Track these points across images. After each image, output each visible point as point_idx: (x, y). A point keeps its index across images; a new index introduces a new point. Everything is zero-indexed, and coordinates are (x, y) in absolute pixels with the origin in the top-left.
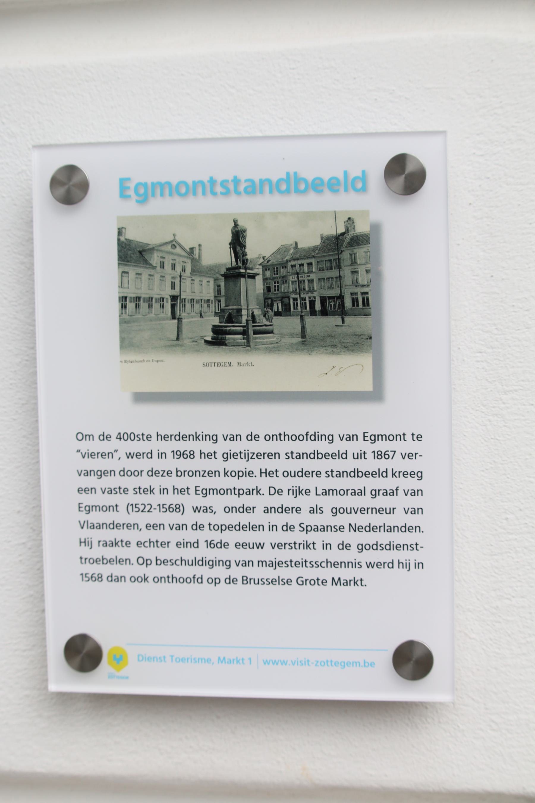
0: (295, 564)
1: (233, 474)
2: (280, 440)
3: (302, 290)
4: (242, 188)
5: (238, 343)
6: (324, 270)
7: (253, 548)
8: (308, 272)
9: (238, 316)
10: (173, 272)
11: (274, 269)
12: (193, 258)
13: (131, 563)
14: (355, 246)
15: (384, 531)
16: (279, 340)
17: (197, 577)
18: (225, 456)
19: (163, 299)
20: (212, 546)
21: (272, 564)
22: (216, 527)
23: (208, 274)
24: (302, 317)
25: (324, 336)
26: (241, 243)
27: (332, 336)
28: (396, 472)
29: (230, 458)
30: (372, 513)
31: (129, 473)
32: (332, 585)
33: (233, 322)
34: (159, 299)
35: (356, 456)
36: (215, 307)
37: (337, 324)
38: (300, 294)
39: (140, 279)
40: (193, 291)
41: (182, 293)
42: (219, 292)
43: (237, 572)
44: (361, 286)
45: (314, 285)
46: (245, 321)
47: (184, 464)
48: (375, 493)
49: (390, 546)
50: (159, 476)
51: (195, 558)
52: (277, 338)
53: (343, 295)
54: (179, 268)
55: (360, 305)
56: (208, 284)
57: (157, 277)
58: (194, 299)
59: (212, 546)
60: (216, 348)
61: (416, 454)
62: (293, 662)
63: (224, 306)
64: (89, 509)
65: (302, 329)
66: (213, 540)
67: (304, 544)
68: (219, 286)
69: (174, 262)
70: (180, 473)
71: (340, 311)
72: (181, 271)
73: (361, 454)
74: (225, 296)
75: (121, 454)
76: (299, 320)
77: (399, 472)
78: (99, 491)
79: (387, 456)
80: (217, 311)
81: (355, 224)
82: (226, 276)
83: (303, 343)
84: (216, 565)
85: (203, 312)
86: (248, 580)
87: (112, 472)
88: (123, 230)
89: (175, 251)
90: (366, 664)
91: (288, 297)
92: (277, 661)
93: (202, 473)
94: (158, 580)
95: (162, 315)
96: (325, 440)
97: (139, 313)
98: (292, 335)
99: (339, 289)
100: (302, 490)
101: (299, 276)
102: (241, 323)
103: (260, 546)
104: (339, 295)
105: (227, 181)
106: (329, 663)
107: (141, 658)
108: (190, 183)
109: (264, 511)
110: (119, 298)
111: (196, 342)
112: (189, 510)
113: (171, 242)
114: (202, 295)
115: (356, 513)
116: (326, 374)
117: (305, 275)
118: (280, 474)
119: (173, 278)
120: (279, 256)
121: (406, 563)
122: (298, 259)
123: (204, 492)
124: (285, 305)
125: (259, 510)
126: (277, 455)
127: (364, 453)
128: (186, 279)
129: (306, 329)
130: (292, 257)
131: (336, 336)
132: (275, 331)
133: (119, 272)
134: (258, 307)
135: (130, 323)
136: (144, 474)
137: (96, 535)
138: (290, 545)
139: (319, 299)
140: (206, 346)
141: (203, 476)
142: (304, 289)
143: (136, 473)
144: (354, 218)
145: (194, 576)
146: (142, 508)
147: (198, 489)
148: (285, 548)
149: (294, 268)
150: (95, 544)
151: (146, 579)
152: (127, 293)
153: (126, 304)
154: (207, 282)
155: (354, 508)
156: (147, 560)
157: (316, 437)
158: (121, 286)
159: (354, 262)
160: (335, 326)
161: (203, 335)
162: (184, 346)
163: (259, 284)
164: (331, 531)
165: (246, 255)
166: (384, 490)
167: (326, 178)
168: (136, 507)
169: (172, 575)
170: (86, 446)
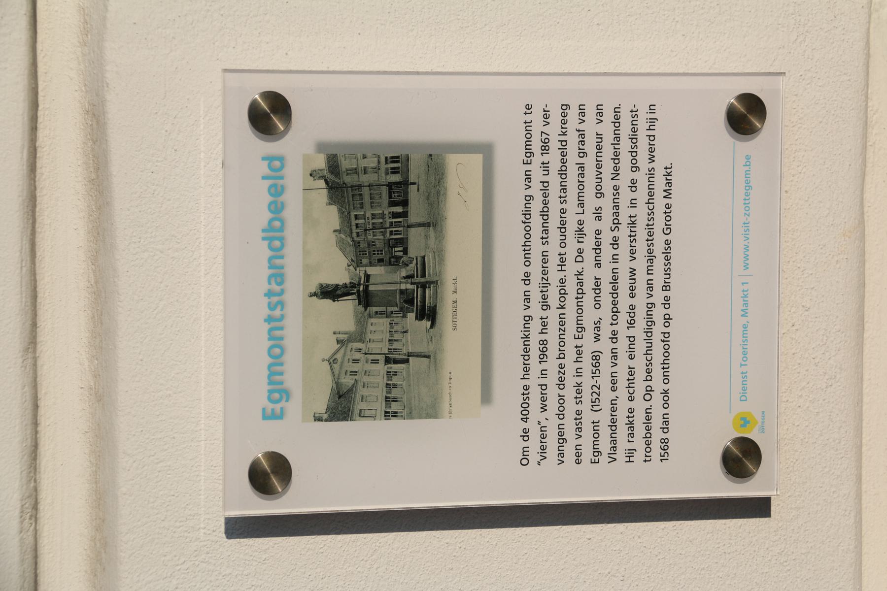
0: (651, 236)
1: (562, 299)
4: (277, 288)
5: (433, 293)
6: (362, 203)
7: (634, 279)
8: (365, 219)
10: (361, 361)
11: (360, 254)
12: (348, 340)
13: (650, 407)
14: (339, 170)
15: (619, 144)
17: (663, 338)
18: (545, 307)
19: (388, 372)
21: (650, 259)
22: (615, 318)
23: (364, 325)
24: (409, 226)
25: (429, 204)
26: (333, 289)
28: (561, 131)
29: (547, 302)
31: (561, 409)
33: (413, 298)
34: (388, 377)
36: (397, 317)
38: (386, 228)
39: (368, 397)
42: (382, 313)
43: (658, 296)
44: (379, 164)
46: (412, 285)
47: (553, 351)
48: (582, 153)
49: (634, 138)
51: (645, 340)
53: (387, 183)
54: (357, 356)
56: (374, 324)
57: (366, 379)
58: (389, 340)
59: (633, 322)
60: (438, 317)
63: (396, 308)
64: (597, 452)
65: (421, 227)
67: (631, 227)
68: (376, 313)
70: (562, 355)
72: (361, 353)
73: (543, 167)
74: (386, 307)
75: (542, 417)
76: (412, 229)
77: (562, 128)
78: (579, 442)
79: (547, 141)
80: (402, 315)
81: (317, 169)
82: (366, 307)
83: (435, 225)
84: (652, 318)
86: (666, 284)
87: (560, 427)
88: (316, 416)
89: (340, 360)
90: (748, 163)
91: (389, 240)
93: (562, 332)
94: (666, 379)
95: (405, 373)
98: (427, 237)
101: (368, 228)
102: (414, 290)
103: (633, 272)
104: (388, 188)
105: (269, 304)
106: (747, 202)
107: (743, 398)
108: (270, 343)
110: (385, 419)
112: (597, 346)
113: (330, 363)
114: (385, 331)
115: (601, 173)
118: (563, 251)
119: (367, 362)
120: (348, 250)
121: (650, 122)
122: (351, 230)
123: (580, 330)
125: (598, 273)
126: (544, 254)
127: (543, 163)
128: (368, 348)
130: (349, 235)
132: (422, 255)
133: (359, 420)
134: (398, 272)
136: (562, 393)
137: (623, 445)
138: (632, 241)
139: (392, 208)
140: (436, 327)
141: (564, 331)
142: (381, 223)
143: (561, 401)
146: (595, 396)
148: (635, 247)
149: (360, 234)
151: (666, 392)
152: (381, 411)
154: (372, 325)
155: (596, 175)
156: (647, 391)
157: (527, 214)
158: (374, 417)
159: (355, 171)
160: (418, 191)
162: (436, 350)
163: (376, 271)
165: (346, 284)
167: (270, 199)
168: (595, 402)
170: (534, 456)
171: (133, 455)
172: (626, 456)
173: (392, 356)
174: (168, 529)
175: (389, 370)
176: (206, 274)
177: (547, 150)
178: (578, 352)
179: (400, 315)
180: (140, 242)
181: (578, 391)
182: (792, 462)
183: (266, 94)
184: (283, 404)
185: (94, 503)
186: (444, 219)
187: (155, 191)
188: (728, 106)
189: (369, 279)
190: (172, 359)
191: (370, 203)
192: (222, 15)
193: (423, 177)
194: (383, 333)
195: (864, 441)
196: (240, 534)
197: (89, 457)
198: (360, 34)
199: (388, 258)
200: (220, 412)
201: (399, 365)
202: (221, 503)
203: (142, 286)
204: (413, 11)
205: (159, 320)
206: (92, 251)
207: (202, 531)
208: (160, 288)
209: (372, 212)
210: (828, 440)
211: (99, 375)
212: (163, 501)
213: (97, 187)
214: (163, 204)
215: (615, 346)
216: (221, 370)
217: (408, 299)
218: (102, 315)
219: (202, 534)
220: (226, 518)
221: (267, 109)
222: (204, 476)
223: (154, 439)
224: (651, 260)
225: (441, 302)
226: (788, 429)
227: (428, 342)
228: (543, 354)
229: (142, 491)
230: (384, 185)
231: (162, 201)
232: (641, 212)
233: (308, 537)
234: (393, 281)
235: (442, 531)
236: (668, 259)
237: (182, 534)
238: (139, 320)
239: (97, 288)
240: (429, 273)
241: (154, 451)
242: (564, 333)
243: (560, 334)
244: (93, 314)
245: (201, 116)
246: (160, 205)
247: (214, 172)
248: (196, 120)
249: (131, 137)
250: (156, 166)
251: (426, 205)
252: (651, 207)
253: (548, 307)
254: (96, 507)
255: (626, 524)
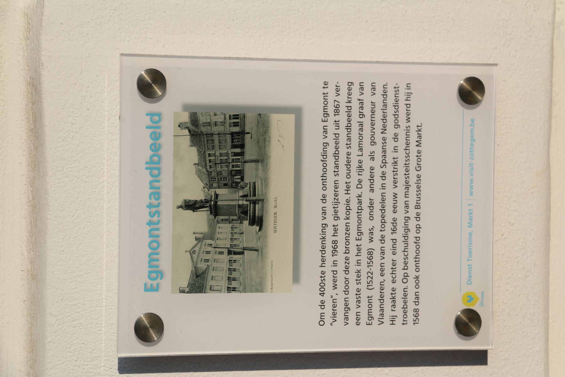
1: (348, 213)
2: (326, 180)
3: (227, 161)
4: (155, 202)
5: (261, 207)
6: (214, 145)
7: (396, 201)
9: (243, 207)
10: (212, 253)
11: (212, 180)
13: (406, 287)
16: (260, 178)
17: (415, 241)
18: (336, 218)
19: (230, 260)
20: (395, 229)
21: (407, 187)
22: (383, 226)
23: (214, 228)
24: (245, 162)
25: (258, 147)
26: (193, 203)
27: (258, 141)
28: (348, 100)
29: (337, 215)
30: (374, 117)
31: (347, 287)
32: (421, 146)
33: (248, 210)
35: (337, 128)
36: (236, 223)
37: (250, 137)
38: (229, 163)
39: (216, 277)
40: (225, 239)
41: (226, 247)
42: (226, 220)
43: (412, 213)
44: (225, 120)
45: (224, 153)
46: (247, 202)
47: (341, 248)
48: (362, 115)
49: (396, 106)
50: (349, 266)
51: (403, 242)
52: (259, 180)
53: (231, 133)
54: (209, 249)
55: (238, 121)
57: (215, 265)
58: (231, 239)
59: (395, 229)
60: (264, 223)
61: (337, 86)
62: (471, 175)
64: (371, 317)
65: (253, 162)
66: (391, 229)
67: (394, 165)
68: (222, 220)
69: (205, 252)
70: (347, 251)
71: (242, 135)
73: (336, 124)
75: (333, 293)
77: (348, 98)
78: (358, 310)
80: (239, 222)
81: (183, 122)
83: (262, 161)
84: (408, 227)
85: (240, 232)
86: (418, 205)
87: (346, 300)
88: (181, 289)
89: (197, 251)
90: (472, 124)
91: (231, 171)
92: (471, 186)
93: (347, 235)
94: (417, 269)
95: (241, 261)
96: (326, 148)
97: (239, 278)
98: (257, 169)
99: (226, 135)
100: (359, 165)
101: (217, 163)
102: (248, 205)
103: (395, 195)
104: (231, 136)
105: (150, 213)
106: (472, 150)
107: (469, 282)
109: (373, 192)
110: (228, 293)
111: (260, 237)
112: (371, 245)
113: (191, 254)
114: (228, 233)
115: (374, 129)
116: (283, 146)
117: (217, 158)
118: (348, 181)
119: (216, 253)
121: (407, 95)
122: (206, 164)
124: (236, 173)
125: (372, 196)
126: (336, 182)
127: (335, 121)
128: (217, 244)
129: (253, 160)
130: (204, 167)
131: (258, 138)
132: (254, 181)
133: (210, 293)
134: (237, 193)
135: (246, 285)
136: (347, 276)
137: (388, 313)
139: (233, 149)
140: (263, 231)
141: (349, 235)
142: (226, 159)
143: (347, 282)
144: (179, 123)
145: (414, 242)
146: (370, 279)
147: (357, 239)
148: (397, 178)
149: (212, 166)
150: (394, 313)
151: (417, 277)
153: (232, 287)
154: (219, 228)
155: (371, 130)
156: (404, 276)
157: (324, 155)
158: (220, 291)
159: (209, 124)
161: (255, 232)
164: (386, 146)
165: (202, 200)
166: (359, 109)
169: (414, 258)
170: (328, 319)
171: (56, 316)
172: (391, 321)
173: (232, 249)
174: (80, 366)
175: (231, 259)
176: (108, 193)
177: (338, 113)
178: (358, 249)
179: (238, 222)
180: (63, 171)
181: (358, 276)
182: (502, 328)
183: (149, 70)
184: (158, 280)
185: (29, 349)
186: (268, 157)
187: (73, 136)
188: (459, 85)
189: (218, 197)
190: (84, 251)
191: (219, 146)
192: (121, 19)
193: (255, 129)
194: (227, 233)
195: (550, 316)
196: (128, 371)
197: (27, 318)
198: (213, 34)
199: (231, 183)
200: (115, 287)
201: (237, 256)
202: (115, 349)
203: (64, 200)
204: (249, 19)
205: (75, 224)
206: (31, 178)
207: (103, 368)
208: (76, 202)
209: (220, 152)
210: (526, 313)
211: (34, 262)
212: (77, 348)
213: (35, 134)
214: (79, 145)
215: (383, 245)
216: (117, 258)
217: (244, 211)
218: (36, 221)
219: (103, 371)
220: (119, 359)
221: (149, 81)
222: (105, 331)
223: (70, 305)
224: (407, 188)
225: (266, 214)
226: (499, 306)
227: (257, 241)
228: (335, 250)
229: (62, 340)
230: (229, 134)
231: (79, 143)
232: (401, 155)
233: (175, 373)
234: (234, 199)
235: (265, 371)
236: (419, 187)
237: (89, 370)
238: (62, 224)
239: (34, 202)
240: (258, 194)
241: (71, 313)
242: (348, 236)
243: (346, 237)
244: (31, 220)
245: (105, 87)
246: (77, 146)
247: (114, 125)
248: (102, 89)
249: (58, 100)
250: (75, 120)
251: (257, 148)
252: (408, 152)
253: (338, 218)
254: (31, 352)
255: (390, 368)
